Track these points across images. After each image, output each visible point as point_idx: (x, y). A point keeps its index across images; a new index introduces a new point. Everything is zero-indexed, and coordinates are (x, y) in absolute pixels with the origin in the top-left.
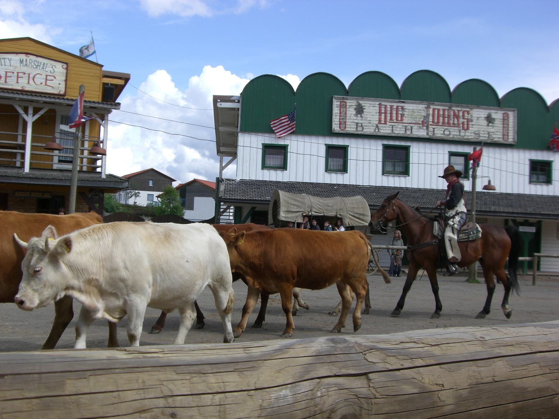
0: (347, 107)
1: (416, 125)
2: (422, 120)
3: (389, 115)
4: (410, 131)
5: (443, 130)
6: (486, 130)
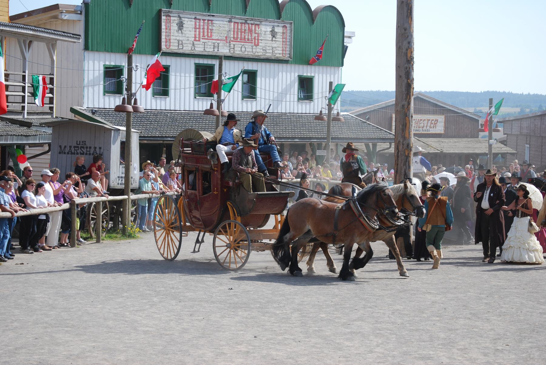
0: (172, 21)
1: (222, 42)
2: (226, 35)
3: (202, 31)
4: (217, 48)
5: (241, 46)
6: (271, 45)
